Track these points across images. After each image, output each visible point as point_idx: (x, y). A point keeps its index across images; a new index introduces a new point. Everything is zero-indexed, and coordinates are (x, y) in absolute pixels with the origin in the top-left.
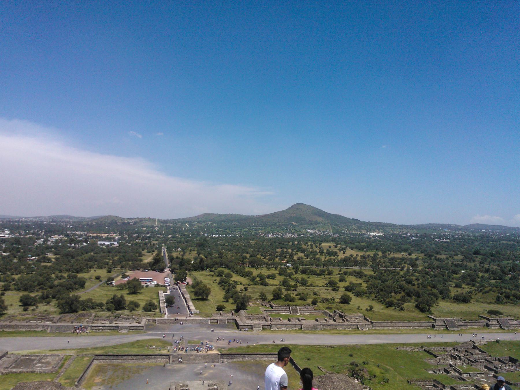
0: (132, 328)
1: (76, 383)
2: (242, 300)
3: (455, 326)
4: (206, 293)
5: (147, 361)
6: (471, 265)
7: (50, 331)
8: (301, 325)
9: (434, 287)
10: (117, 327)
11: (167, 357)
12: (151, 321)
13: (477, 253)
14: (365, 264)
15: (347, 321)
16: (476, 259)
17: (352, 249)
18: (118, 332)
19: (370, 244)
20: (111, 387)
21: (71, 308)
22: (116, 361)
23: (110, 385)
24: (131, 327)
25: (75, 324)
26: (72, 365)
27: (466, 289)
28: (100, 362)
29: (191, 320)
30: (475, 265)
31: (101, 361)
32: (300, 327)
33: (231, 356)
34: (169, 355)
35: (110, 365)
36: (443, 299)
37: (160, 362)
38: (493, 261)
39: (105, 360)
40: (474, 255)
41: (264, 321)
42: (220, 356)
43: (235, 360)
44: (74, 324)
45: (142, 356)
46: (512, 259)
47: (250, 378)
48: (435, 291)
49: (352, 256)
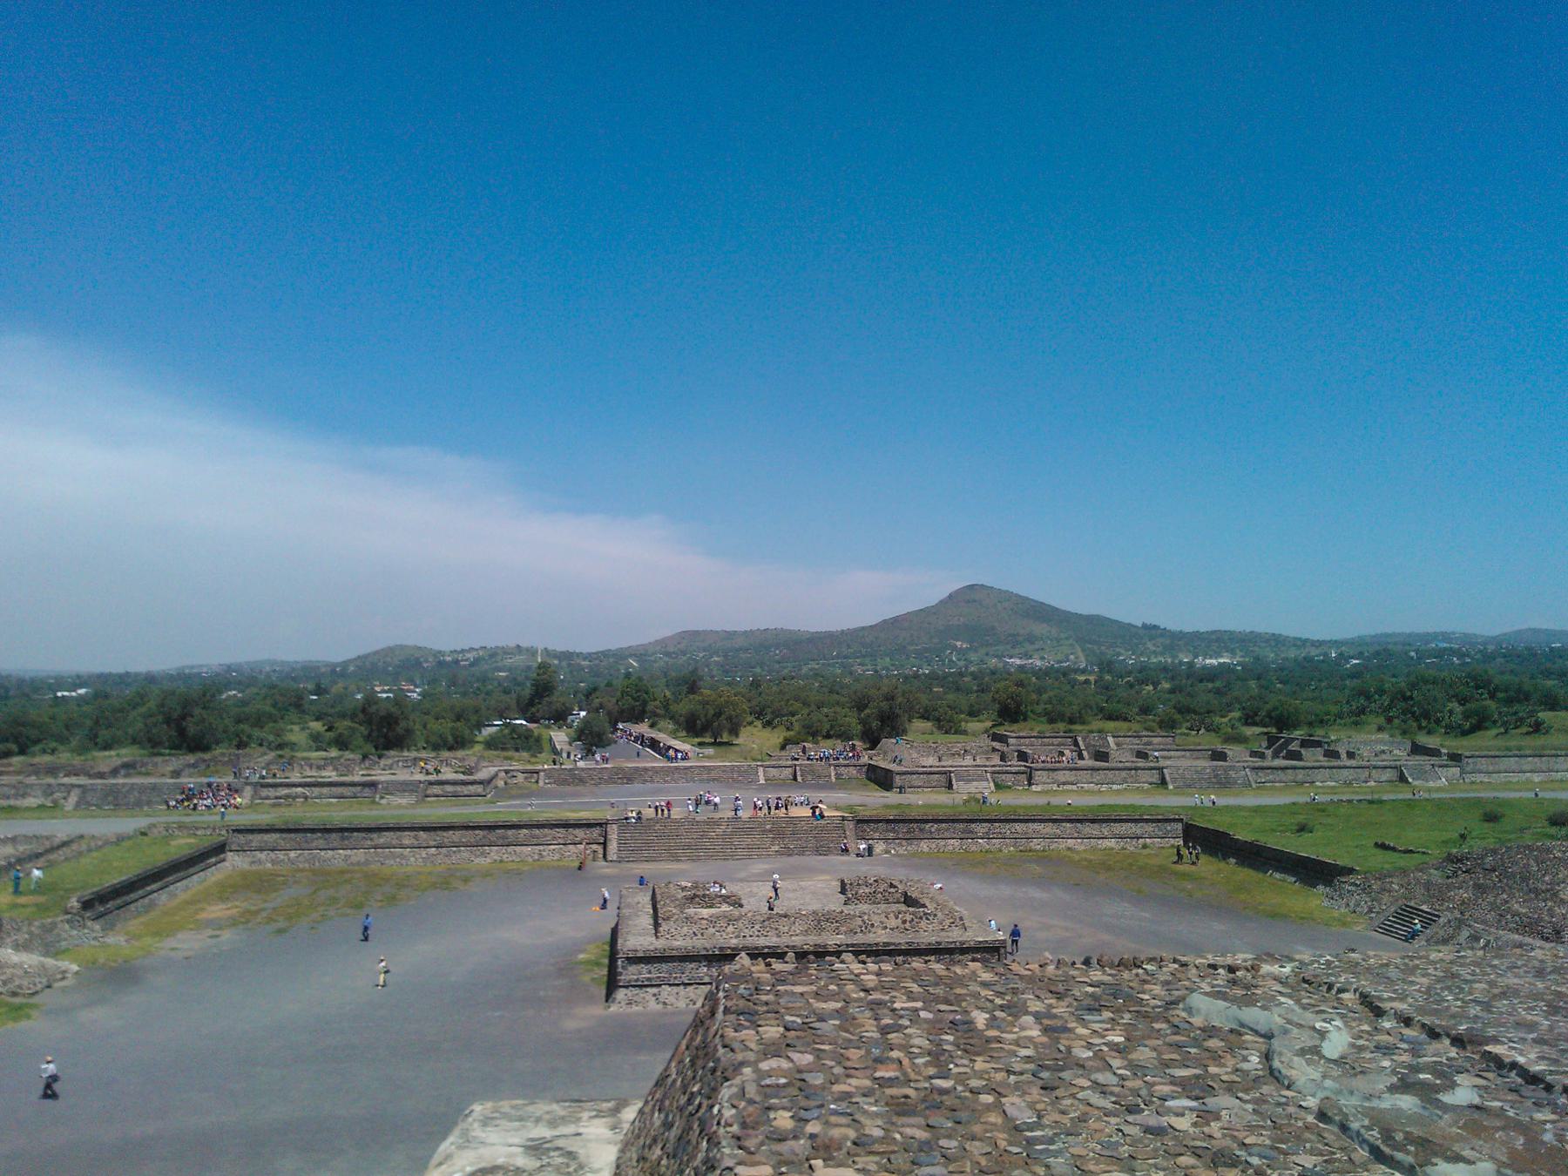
0: (436, 790)
1: (74, 903)
2: (885, 705)
4: (730, 718)
5: (495, 853)
7: (78, 805)
8: (1161, 769)
10: (373, 785)
11: (596, 832)
12: (521, 777)
15: (1351, 755)
18: (374, 802)
20: (280, 931)
21: (182, 732)
22: (338, 858)
23: (281, 924)
24: (431, 783)
25: (190, 781)
26: (95, 854)
28: (260, 862)
29: (686, 768)
31: (262, 856)
32: (1155, 778)
33: (903, 828)
34: (603, 825)
35: (302, 870)
37: (559, 853)
39: (281, 855)
41: (996, 760)
42: (850, 825)
43: (924, 846)
44: (183, 780)
45: (467, 828)
47: (1037, 894)
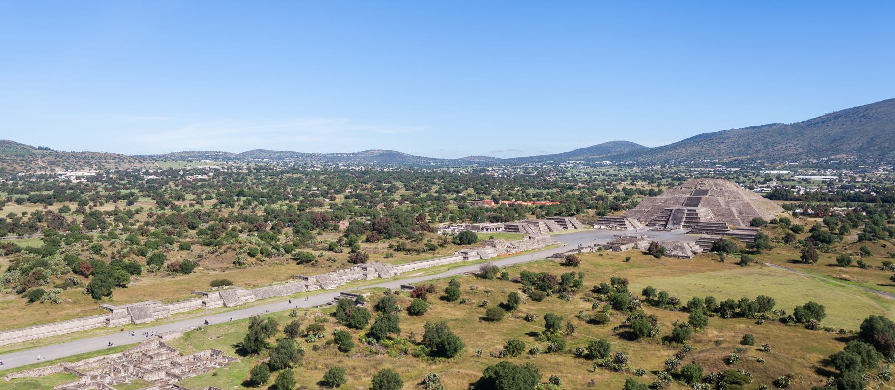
3: (147, 316)
6: (225, 213)
9: (142, 253)
13: (240, 194)
14: (32, 228)
16: (237, 204)
17: (19, 202)
19: (61, 192)
27: (197, 249)
30: (231, 213)
36: (150, 271)
38: (262, 204)
40: (235, 198)
46: (289, 198)
48: (142, 261)
49: (11, 216)
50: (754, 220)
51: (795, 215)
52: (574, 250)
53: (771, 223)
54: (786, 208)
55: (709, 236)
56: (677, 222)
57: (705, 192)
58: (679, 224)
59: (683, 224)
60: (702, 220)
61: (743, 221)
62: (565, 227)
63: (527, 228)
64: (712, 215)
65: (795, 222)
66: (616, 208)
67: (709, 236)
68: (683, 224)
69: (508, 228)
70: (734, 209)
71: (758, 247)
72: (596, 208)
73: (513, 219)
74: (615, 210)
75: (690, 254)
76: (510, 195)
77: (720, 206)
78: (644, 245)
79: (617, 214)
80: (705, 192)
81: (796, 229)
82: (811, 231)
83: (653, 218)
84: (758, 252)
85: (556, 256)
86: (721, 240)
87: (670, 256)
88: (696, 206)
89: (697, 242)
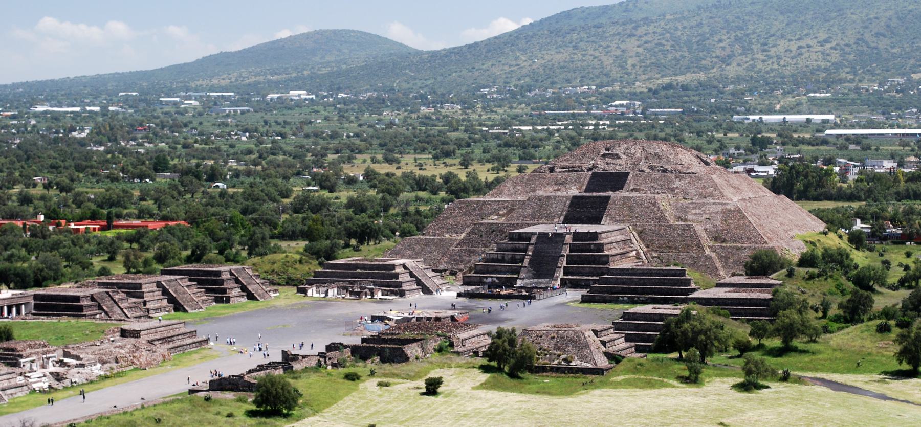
50: (756, 258)
51: (856, 240)
52: (273, 365)
53: (806, 261)
54: (832, 223)
55: (648, 309)
56: (543, 267)
57: (617, 180)
58: (550, 275)
59: (560, 274)
60: (615, 265)
61: (725, 259)
62: (221, 297)
63: (107, 304)
64: (638, 245)
65: (860, 258)
66: (365, 235)
67: (648, 309)
68: (560, 274)
69: (48, 306)
70: (699, 228)
71: (788, 332)
72: (307, 235)
73: (57, 279)
74: (361, 242)
75: (603, 362)
76: (25, 200)
77: (662, 218)
78: (477, 337)
79: (371, 253)
80: (617, 180)
81: (865, 282)
82: (902, 283)
83: (476, 260)
84: (785, 350)
85: (220, 384)
86: (687, 316)
87: (542, 369)
88: (597, 221)
89: (618, 327)
